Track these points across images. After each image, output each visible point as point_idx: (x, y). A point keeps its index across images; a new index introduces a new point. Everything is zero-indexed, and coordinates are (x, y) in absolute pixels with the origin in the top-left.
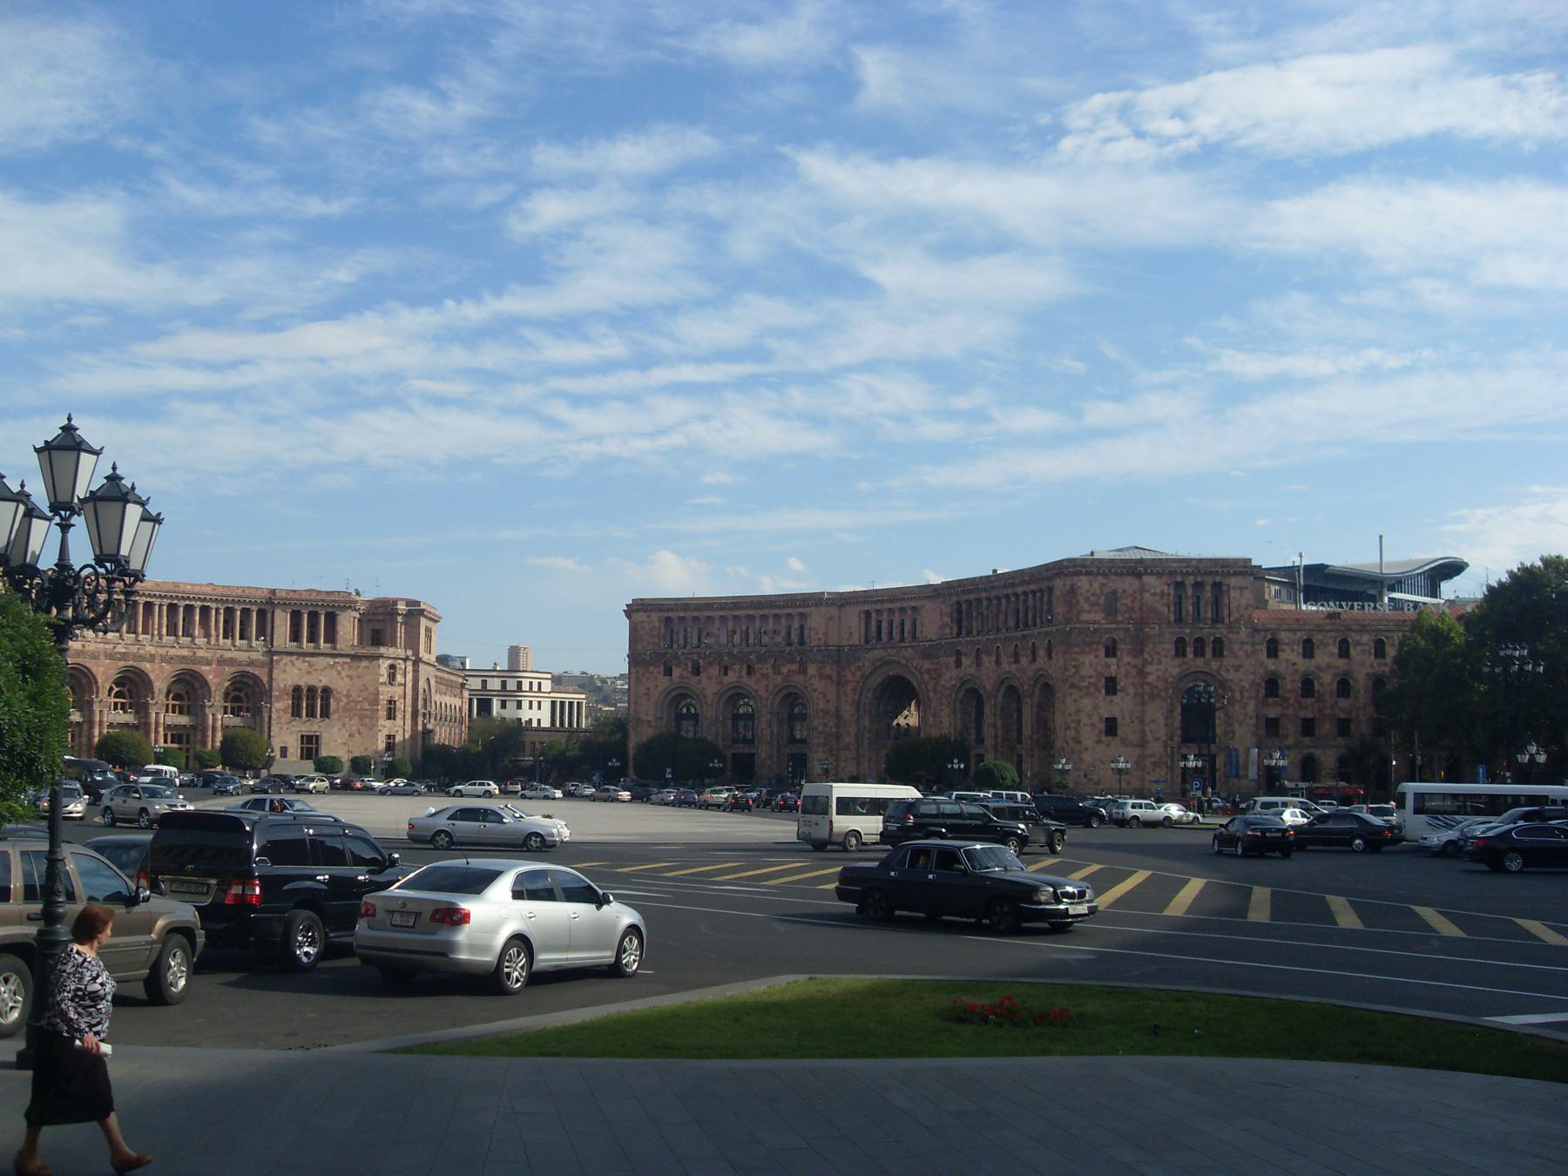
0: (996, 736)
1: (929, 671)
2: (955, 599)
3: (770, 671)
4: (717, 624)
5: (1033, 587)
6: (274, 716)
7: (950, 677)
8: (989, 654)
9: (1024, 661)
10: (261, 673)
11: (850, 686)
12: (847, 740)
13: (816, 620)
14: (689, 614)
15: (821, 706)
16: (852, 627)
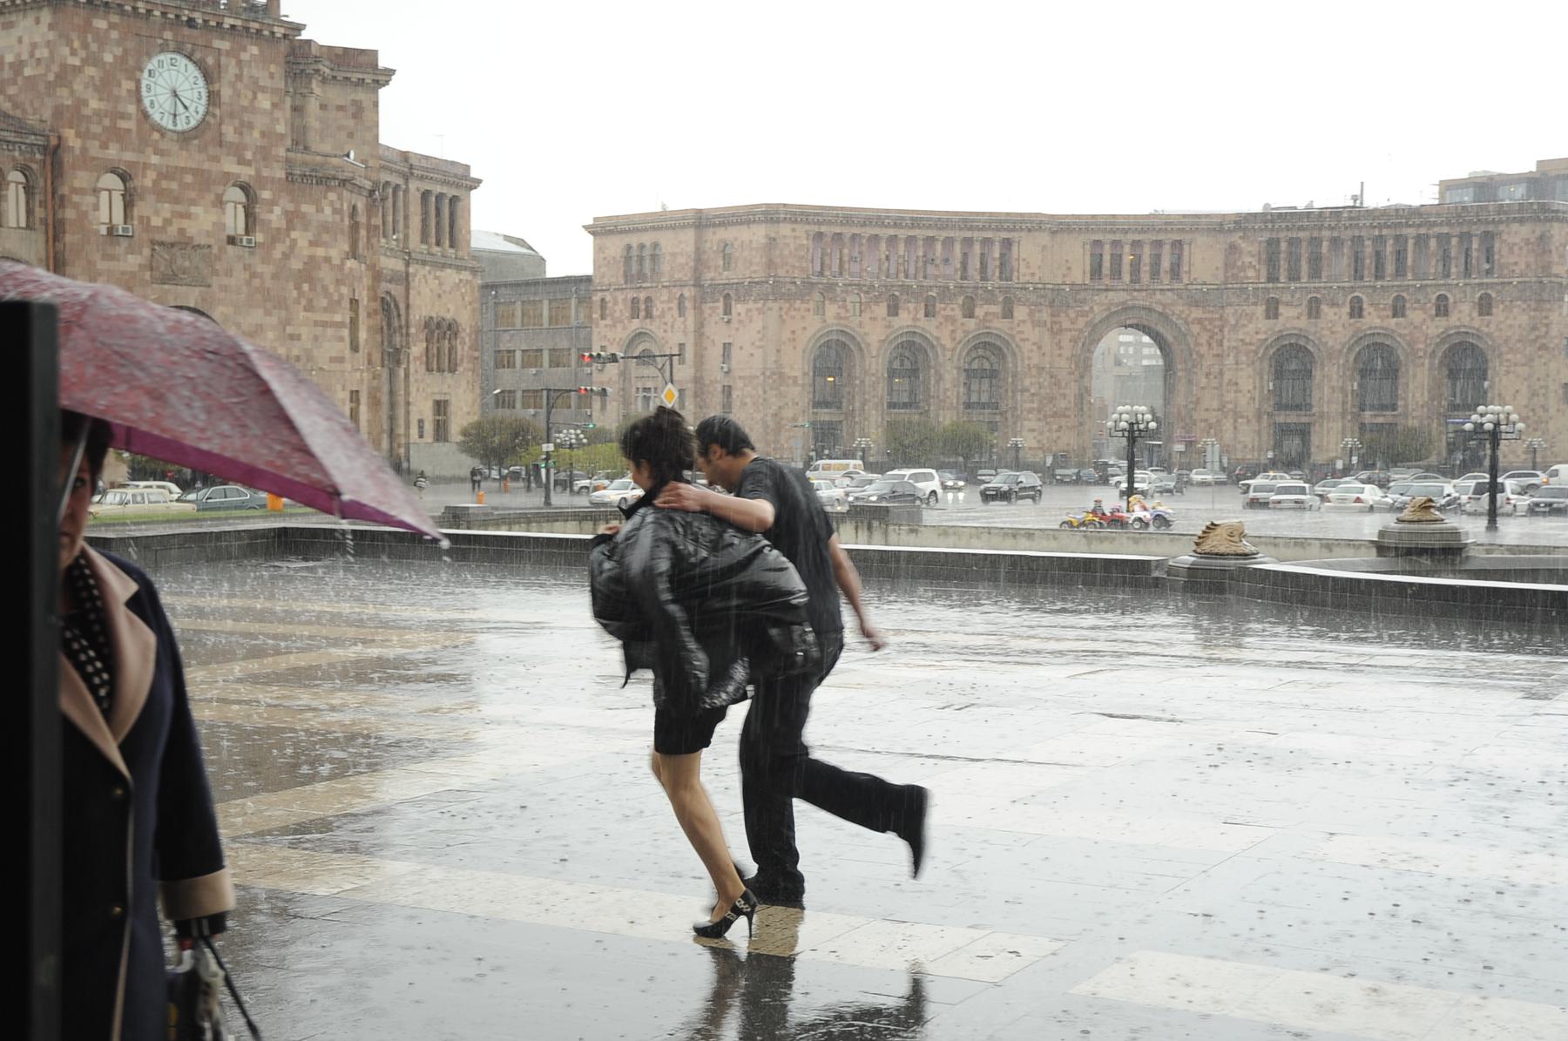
0: (1344, 403)
1: (1200, 321)
2: (1266, 236)
3: (958, 313)
4: (883, 245)
5: (1445, 230)
6: (412, 370)
7: (1257, 328)
8: (1333, 304)
9: (1415, 316)
10: (397, 290)
11: (1067, 336)
12: (1063, 404)
13: (1028, 252)
14: (848, 231)
15: (1035, 361)
16: (1075, 261)
